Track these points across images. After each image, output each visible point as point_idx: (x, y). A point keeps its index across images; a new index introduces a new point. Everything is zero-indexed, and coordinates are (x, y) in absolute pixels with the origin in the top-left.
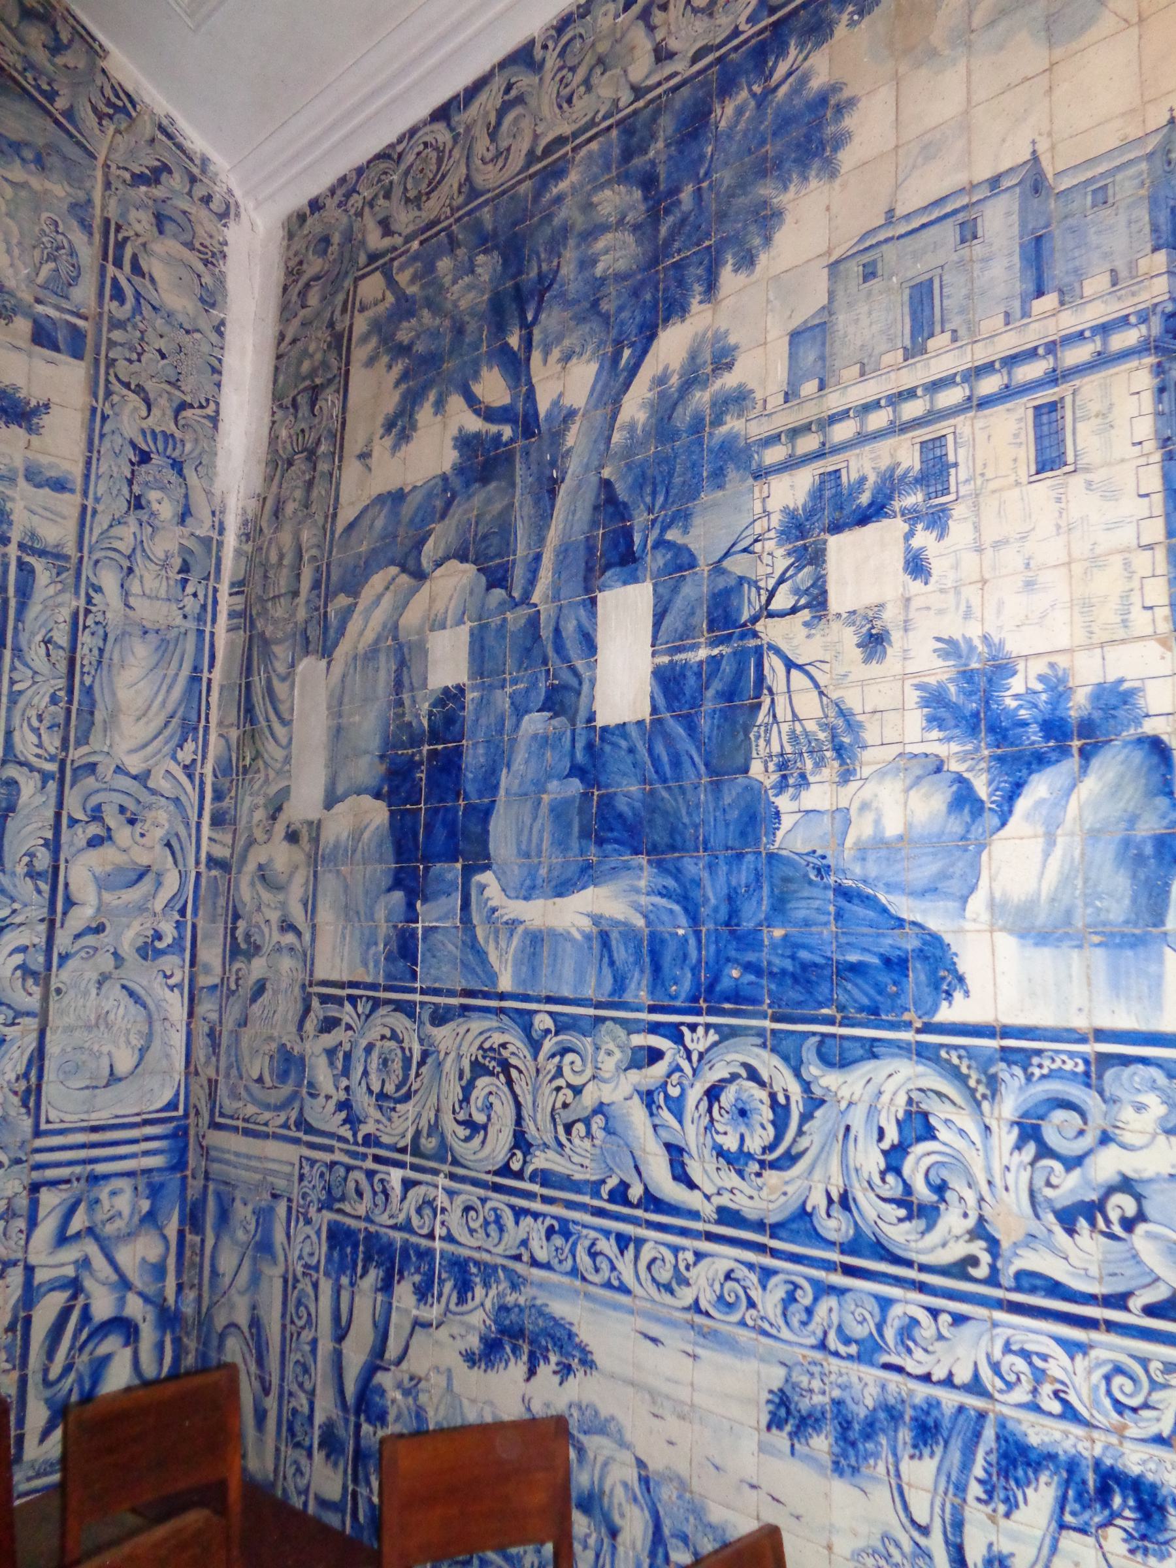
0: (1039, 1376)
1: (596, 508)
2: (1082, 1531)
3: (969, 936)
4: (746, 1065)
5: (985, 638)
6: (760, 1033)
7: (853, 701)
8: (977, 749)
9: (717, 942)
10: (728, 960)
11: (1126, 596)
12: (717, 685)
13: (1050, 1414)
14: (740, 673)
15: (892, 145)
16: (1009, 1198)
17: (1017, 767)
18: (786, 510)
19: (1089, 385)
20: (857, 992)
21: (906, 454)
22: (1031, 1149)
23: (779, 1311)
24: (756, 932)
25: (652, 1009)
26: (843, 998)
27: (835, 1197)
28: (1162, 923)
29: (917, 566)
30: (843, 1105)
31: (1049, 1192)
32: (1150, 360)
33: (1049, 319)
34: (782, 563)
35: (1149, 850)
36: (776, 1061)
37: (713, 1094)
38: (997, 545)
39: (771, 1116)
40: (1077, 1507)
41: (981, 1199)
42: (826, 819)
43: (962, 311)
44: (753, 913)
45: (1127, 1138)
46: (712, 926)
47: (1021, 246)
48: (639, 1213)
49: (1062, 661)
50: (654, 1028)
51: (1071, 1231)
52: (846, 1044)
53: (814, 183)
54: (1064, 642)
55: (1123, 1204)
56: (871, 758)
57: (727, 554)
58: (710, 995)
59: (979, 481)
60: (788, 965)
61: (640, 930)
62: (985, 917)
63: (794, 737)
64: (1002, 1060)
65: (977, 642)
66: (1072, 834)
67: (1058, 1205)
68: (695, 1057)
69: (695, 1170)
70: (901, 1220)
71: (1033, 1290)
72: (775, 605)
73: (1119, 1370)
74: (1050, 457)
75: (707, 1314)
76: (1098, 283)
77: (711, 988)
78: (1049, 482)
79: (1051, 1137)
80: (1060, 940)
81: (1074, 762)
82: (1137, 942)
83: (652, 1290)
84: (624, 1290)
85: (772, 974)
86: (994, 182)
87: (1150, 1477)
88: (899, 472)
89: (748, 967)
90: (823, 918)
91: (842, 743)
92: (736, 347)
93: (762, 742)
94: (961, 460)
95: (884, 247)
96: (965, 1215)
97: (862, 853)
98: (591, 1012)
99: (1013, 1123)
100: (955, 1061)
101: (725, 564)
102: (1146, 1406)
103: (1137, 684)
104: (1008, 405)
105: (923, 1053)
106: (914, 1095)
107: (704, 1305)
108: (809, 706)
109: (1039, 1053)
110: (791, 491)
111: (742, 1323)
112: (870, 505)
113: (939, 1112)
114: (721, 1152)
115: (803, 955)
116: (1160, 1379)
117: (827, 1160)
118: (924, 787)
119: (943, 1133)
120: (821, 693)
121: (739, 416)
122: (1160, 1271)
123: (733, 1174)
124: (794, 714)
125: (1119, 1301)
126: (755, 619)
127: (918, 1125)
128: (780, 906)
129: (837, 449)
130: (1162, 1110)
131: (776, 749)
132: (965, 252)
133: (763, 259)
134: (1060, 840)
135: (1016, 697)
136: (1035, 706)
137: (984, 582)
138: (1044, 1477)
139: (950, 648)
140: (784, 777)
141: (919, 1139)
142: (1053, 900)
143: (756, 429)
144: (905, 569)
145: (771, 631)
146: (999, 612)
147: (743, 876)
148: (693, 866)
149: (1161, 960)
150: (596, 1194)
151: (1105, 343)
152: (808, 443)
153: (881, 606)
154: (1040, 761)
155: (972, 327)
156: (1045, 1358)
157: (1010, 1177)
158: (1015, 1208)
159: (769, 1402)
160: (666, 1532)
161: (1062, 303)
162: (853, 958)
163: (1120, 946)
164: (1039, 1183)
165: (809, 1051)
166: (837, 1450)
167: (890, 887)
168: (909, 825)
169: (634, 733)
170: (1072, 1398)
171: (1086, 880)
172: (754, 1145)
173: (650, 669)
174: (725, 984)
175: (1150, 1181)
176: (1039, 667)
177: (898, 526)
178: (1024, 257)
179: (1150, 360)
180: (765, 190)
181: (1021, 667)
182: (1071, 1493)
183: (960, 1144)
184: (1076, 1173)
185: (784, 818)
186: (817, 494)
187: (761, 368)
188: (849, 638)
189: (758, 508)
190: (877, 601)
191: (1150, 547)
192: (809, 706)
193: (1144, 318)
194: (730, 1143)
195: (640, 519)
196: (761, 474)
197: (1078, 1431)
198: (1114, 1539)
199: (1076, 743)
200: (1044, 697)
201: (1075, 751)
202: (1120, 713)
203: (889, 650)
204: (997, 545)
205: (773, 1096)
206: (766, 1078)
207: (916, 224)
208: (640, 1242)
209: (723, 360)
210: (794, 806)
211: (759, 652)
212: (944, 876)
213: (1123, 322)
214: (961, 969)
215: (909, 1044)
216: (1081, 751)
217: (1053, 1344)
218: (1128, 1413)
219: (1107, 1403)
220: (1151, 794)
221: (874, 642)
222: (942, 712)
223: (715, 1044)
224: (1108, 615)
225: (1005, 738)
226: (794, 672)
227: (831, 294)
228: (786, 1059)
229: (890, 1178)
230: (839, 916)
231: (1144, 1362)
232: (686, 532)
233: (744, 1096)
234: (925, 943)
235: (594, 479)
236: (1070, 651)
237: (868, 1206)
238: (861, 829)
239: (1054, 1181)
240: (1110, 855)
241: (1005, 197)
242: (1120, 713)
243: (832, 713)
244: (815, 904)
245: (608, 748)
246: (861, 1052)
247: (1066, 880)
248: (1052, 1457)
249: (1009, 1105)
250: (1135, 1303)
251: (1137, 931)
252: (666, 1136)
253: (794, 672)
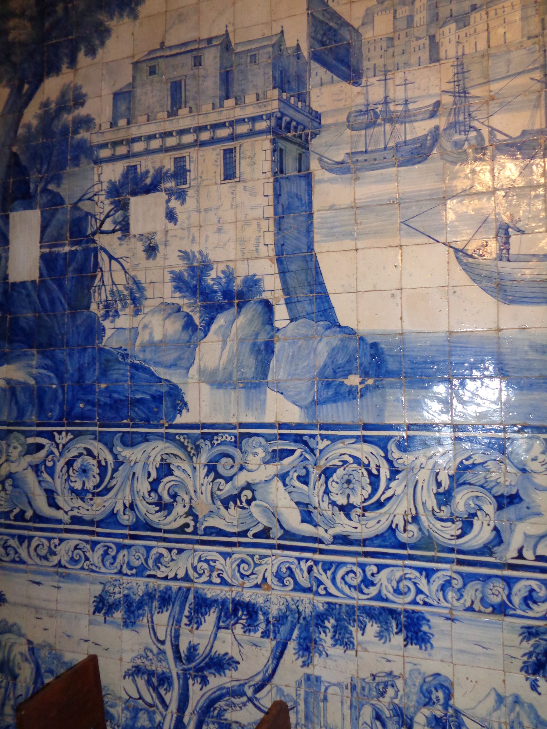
0: (212, 569)
1: (9, 167)
2: (226, 628)
3: (190, 385)
4: (86, 449)
5: (200, 252)
6: (94, 433)
7: (141, 277)
8: (195, 302)
9: (73, 391)
10: (78, 399)
11: (258, 239)
12: (74, 265)
13: (216, 584)
14: (87, 259)
15: (164, 9)
16: (203, 497)
17: (212, 310)
18: (110, 182)
19: (247, 143)
20: (139, 412)
21: (167, 163)
22: (212, 475)
23: (100, 560)
24: (92, 386)
25: (38, 425)
26: (133, 415)
27: (127, 505)
28: (267, 378)
29: (171, 216)
30: (132, 463)
31: (219, 493)
32: (270, 137)
33: (231, 111)
34: (108, 208)
35: (262, 347)
36: (101, 446)
37: (70, 464)
38: (206, 210)
39: (98, 471)
40: (225, 619)
41: (191, 498)
42: (127, 332)
43: (194, 99)
44: (90, 377)
45: (250, 467)
46: (70, 383)
47: (221, 74)
48: (30, 524)
49: (232, 265)
50: (40, 434)
51: (227, 508)
52: (134, 436)
53: (126, 19)
54: (232, 257)
55: (248, 494)
56: (149, 304)
57: (80, 200)
58: (69, 417)
59: (199, 180)
60: (108, 401)
61: (33, 386)
62: (196, 377)
63: (112, 293)
64: (202, 438)
65: (197, 254)
66: (233, 341)
67: (222, 498)
68: (61, 447)
69: (60, 500)
70: (157, 512)
71: (211, 534)
72: (105, 227)
73: (243, 561)
74: (229, 174)
75: (65, 567)
76: (250, 98)
77: (69, 413)
78: (229, 185)
79: (220, 469)
80: (227, 386)
81: (235, 309)
82: (256, 386)
83: (37, 560)
84: (22, 562)
85: (100, 406)
86: (209, 40)
87: (253, 601)
88: (164, 170)
89: (88, 402)
90: (125, 378)
91: (135, 296)
92: (85, 95)
93: (96, 294)
94: (192, 169)
95: (160, 60)
96: (184, 506)
97: (144, 348)
98: (5, 428)
99: (205, 465)
100: (182, 440)
101: (80, 205)
102: (252, 574)
103: (261, 277)
104: (213, 147)
105: (169, 438)
106: (164, 457)
107: (63, 563)
108: (120, 278)
109: (217, 434)
110: (113, 172)
111: (82, 568)
112: (151, 184)
113: (174, 463)
114: (73, 490)
115: (115, 396)
116: (258, 562)
117: (124, 490)
118: (172, 319)
119: (176, 472)
120: (126, 272)
121: (87, 131)
122: (260, 519)
123: (79, 500)
124: (113, 282)
125: (244, 534)
126: (94, 234)
127: (165, 469)
128: (104, 373)
129: (135, 155)
130: (263, 454)
131: (103, 298)
132: (196, 71)
133: (100, 52)
134: (228, 343)
135: (213, 279)
136: (221, 284)
137: (201, 226)
138: (212, 610)
139: (185, 256)
140: (107, 312)
141: (166, 476)
142: (225, 369)
143: (96, 139)
144: (166, 217)
145: (102, 240)
146: (206, 241)
147: (86, 359)
148: (61, 354)
149: (265, 393)
150: (8, 518)
151: (253, 126)
152: (122, 150)
153: (155, 233)
154: (221, 308)
155: (199, 108)
156: (215, 561)
157: (203, 488)
158: (205, 501)
159: (94, 601)
160: (43, 671)
161: (236, 104)
162: (138, 396)
163: (250, 388)
164: (215, 489)
165: (117, 441)
166: (125, 616)
167: (156, 364)
168: (165, 335)
169: (30, 287)
170: (225, 576)
171: (238, 360)
172: (89, 486)
173: (38, 255)
174: (76, 411)
175: (257, 484)
176: (222, 267)
177: (163, 196)
178: (221, 79)
179: (270, 137)
180: (102, 17)
181: (215, 266)
182: (223, 614)
183: (183, 476)
184: (230, 484)
185: (107, 331)
186: (125, 175)
187: (98, 107)
188: (140, 247)
189: (96, 179)
190: (153, 231)
191: (268, 219)
192: (120, 278)
193: (269, 117)
194: (78, 486)
195: (34, 176)
196: (98, 162)
197: (226, 588)
198: (238, 630)
199: (236, 301)
200: (224, 280)
201: (235, 305)
202: (254, 289)
203: (158, 254)
204: (206, 210)
205: (99, 462)
206: (96, 454)
207: (174, 52)
208: (31, 538)
209: (79, 100)
210: (112, 325)
211: (96, 251)
212: (180, 358)
213: (261, 118)
214: (186, 399)
215: (162, 434)
216: (238, 304)
217: (218, 555)
218: (246, 578)
219: (238, 575)
220: (264, 324)
221: (151, 250)
222: (181, 285)
223: (71, 440)
224: (251, 246)
225: (207, 298)
226: (113, 261)
227: (134, 78)
228: (106, 444)
229: (153, 494)
230: (132, 377)
231: (252, 556)
232: (58, 185)
233: (85, 464)
234: (171, 389)
235: (7, 151)
236: (235, 261)
237: (142, 507)
238: (143, 337)
239: (221, 488)
240: (248, 350)
241: (214, 48)
242: (254, 289)
243: (131, 282)
244: (121, 372)
245: (15, 294)
246: (140, 439)
247: (230, 361)
248: (216, 601)
249: (204, 458)
250: (250, 534)
251: (257, 382)
252: (44, 485)
253: (113, 261)
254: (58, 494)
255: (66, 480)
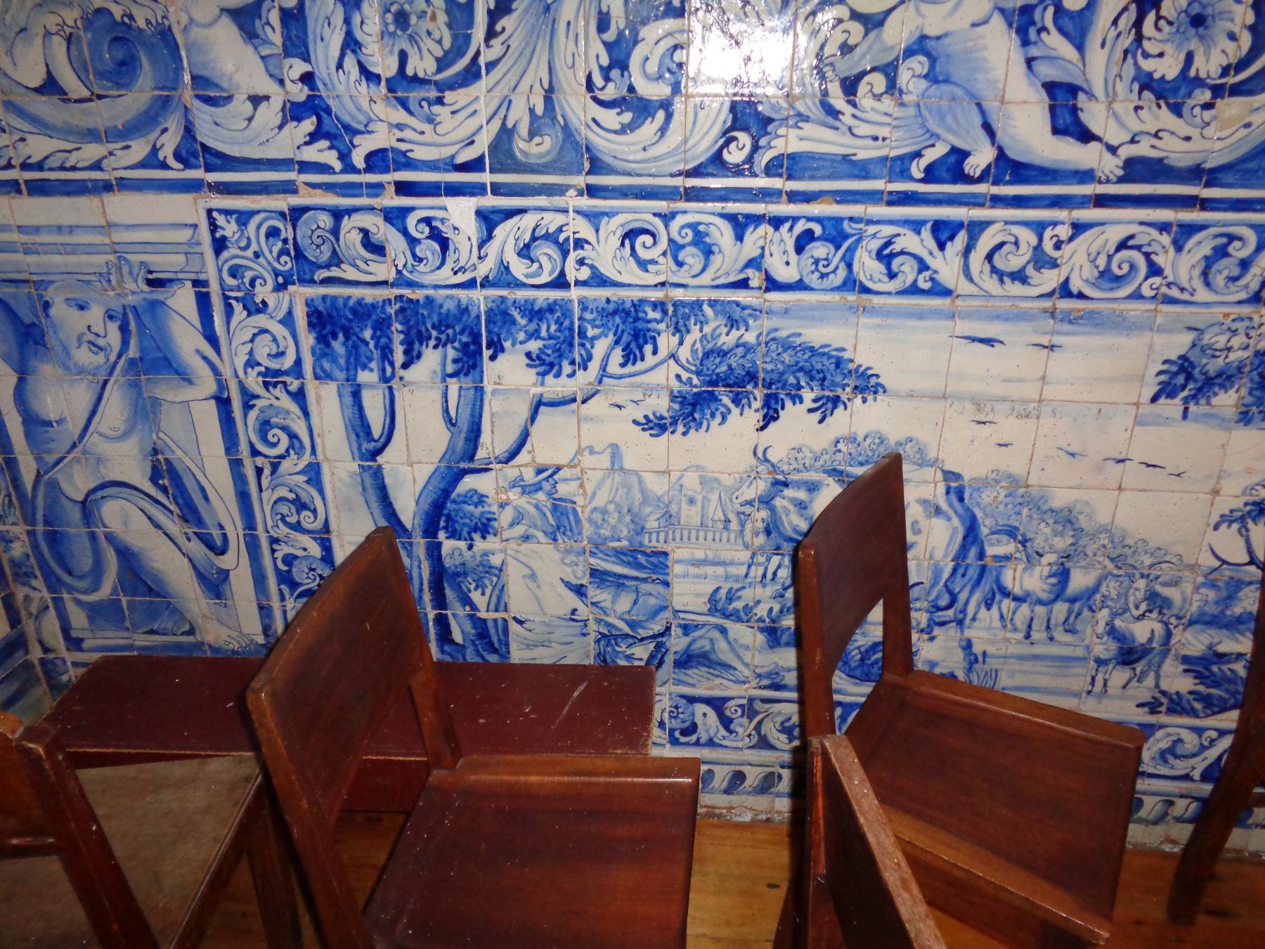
23: (1197, 272)
39: (1250, 18)
48: (981, 188)
69: (1094, 115)
75: (1081, 296)
83: (991, 284)
84: (940, 291)
107: (1075, 286)
111: (1137, 296)
114: (1147, 83)
150: (905, 175)
159: (1160, 373)
160: (984, 531)
166: (1249, 400)
172: (1209, 65)
194: (1168, 68)
208: (976, 229)
254: (1091, 96)
255: (1126, 52)
